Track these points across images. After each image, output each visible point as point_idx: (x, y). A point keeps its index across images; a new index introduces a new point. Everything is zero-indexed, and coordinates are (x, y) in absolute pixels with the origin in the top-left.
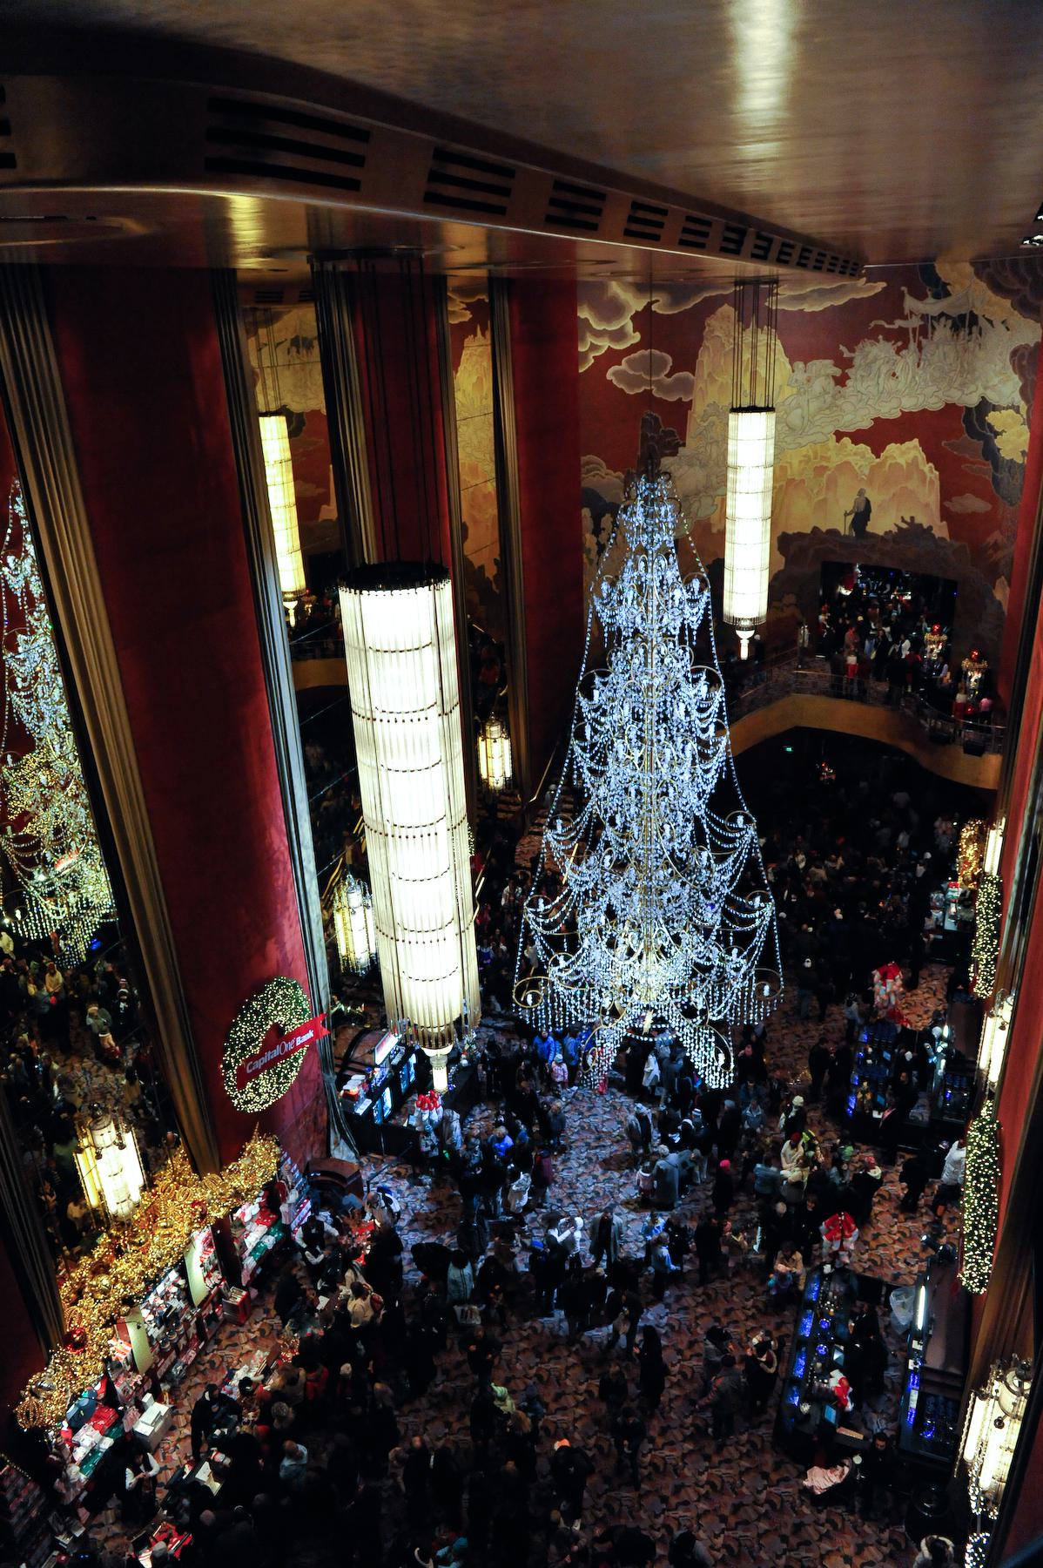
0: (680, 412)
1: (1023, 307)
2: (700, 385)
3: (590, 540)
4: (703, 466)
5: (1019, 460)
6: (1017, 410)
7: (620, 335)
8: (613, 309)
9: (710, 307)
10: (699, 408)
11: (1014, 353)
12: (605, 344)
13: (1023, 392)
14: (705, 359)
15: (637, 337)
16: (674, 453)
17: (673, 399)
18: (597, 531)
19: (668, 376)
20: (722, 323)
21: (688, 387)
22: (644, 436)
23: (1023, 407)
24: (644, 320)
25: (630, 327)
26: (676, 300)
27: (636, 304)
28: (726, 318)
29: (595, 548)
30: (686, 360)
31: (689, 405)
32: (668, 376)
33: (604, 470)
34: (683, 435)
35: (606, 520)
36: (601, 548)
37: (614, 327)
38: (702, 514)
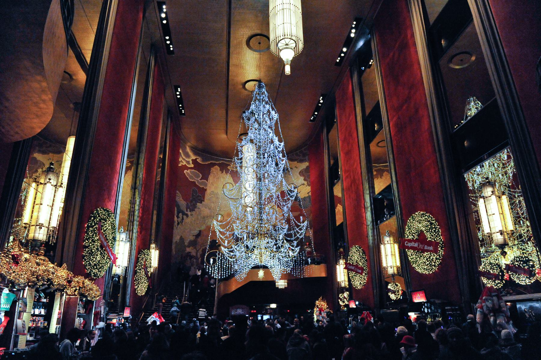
0: (203, 191)
1: (301, 161)
2: (209, 185)
3: (176, 219)
4: (210, 209)
5: (307, 195)
6: (304, 184)
7: (188, 162)
8: (188, 156)
9: (213, 165)
10: (208, 192)
11: (300, 172)
12: (185, 163)
13: (305, 180)
14: (211, 178)
15: (192, 166)
16: (201, 203)
17: (202, 187)
18: (178, 217)
19: (201, 179)
20: (216, 170)
21: (206, 185)
22: (193, 195)
23: (306, 183)
24: (194, 161)
25: (191, 162)
26: (203, 161)
27: (194, 157)
28: (217, 169)
29: (177, 222)
30: (205, 177)
31: (206, 190)
32: (201, 179)
33: (181, 199)
34: (204, 198)
35: (180, 215)
36: (178, 224)
37: (187, 160)
38: (209, 224)
